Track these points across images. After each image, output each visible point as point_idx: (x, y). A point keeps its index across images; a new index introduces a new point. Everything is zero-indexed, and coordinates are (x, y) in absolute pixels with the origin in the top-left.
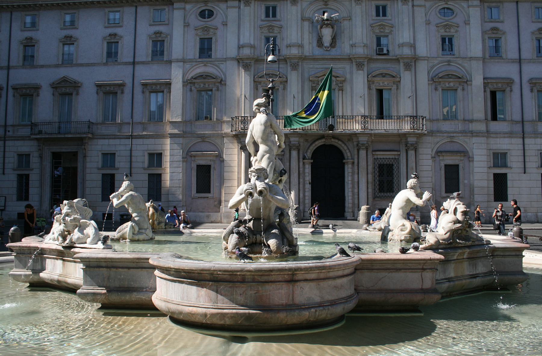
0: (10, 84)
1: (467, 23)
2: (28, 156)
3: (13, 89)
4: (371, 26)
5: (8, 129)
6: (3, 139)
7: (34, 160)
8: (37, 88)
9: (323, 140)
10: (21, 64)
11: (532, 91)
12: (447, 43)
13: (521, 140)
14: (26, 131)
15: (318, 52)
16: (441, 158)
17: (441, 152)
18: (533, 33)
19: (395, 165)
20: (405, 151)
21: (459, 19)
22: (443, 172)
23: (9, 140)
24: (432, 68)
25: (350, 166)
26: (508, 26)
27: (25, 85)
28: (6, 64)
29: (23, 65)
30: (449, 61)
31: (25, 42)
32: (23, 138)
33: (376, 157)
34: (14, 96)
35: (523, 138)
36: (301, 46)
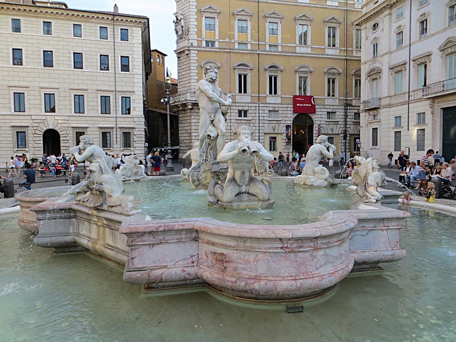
0: (411, 58)
2: (424, 113)
3: (413, 61)
5: (410, 95)
6: (407, 103)
7: (428, 117)
8: (429, 55)
10: (418, 38)
14: (420, 94)
23: (411, 103)
27: (420, 55)
28: (409, 43)
29: (420, 38)
31: (420, 19)
32: (420, 100)
34: (414, 67)
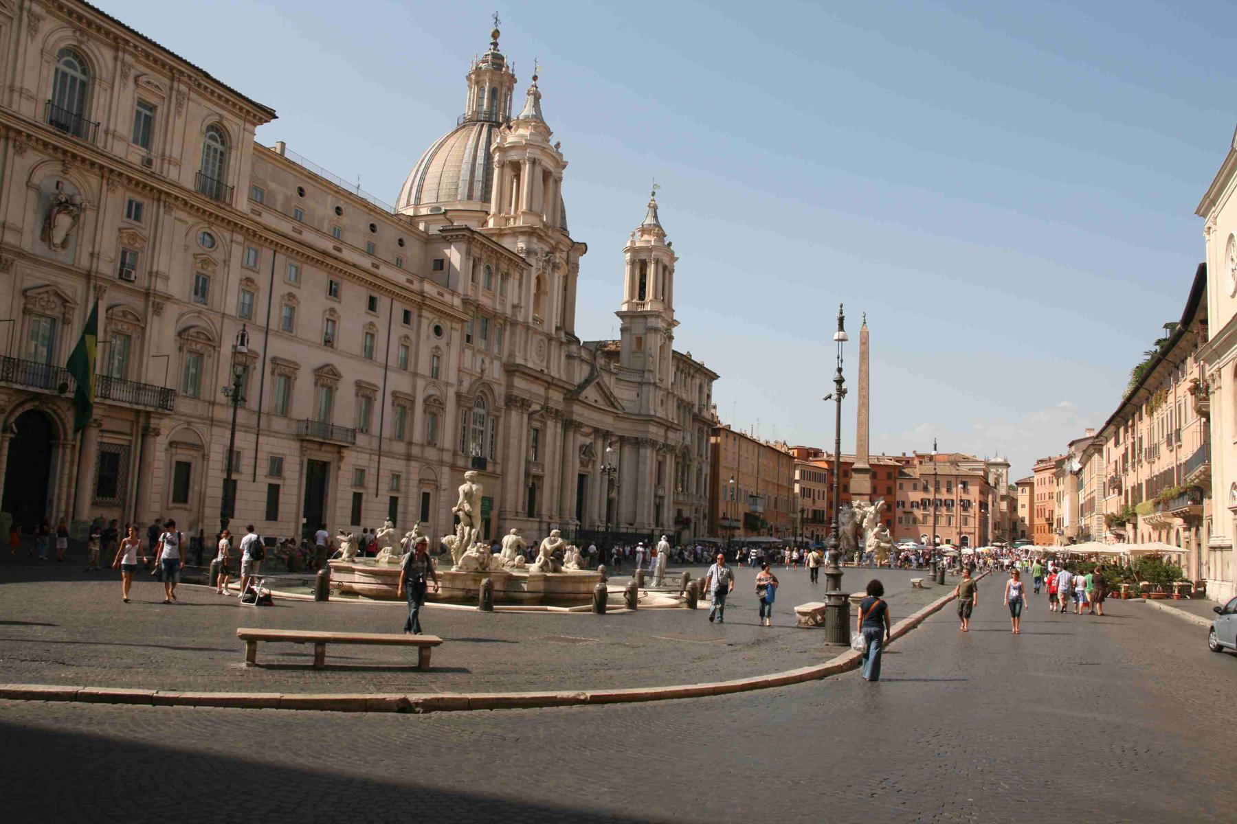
1: (226, 262)
4: (120, 230)
9: (37, 403)
11: (273, 373)
12: (201, 288)
13: (253, 437)
15: (40, 249)
16: (174, 451)
18: (283, 297)
21: (218, 255)
22: (173, 472)
24: (181, 316)
25: (68, 451)
26: (262, 280)
30: (200, 312)
36: (20, 232)
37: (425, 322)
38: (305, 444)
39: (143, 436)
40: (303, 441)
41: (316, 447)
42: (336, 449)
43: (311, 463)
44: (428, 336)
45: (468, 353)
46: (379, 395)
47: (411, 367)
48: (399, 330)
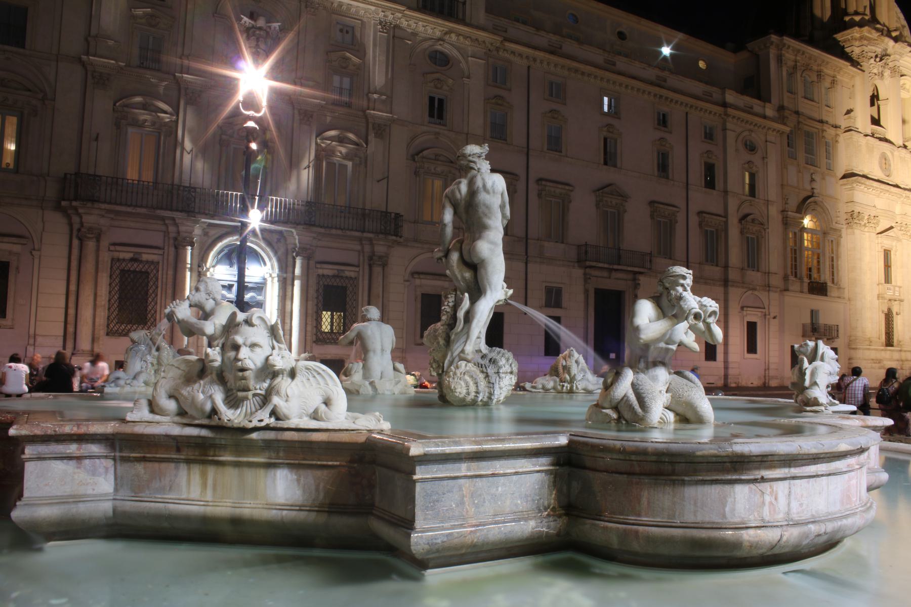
13: (522, 265)
16: (418, 282)
17: (418, 273)
19: (351, 289)
20: (367, 267)
22: (419, 306)
30: (437, 134)
33: (320, 272)
35: (526, 264)
37: (731, 136)
38: (588, 270)
39: (370, 266)
40: (587, 267)
41: (605, 274)
42: (630, 276)
43: (598, 292)
44: (737, 150)
45: (792, 170)
46: (681, 217)
47: (719, 184)
48: (698, 147)
